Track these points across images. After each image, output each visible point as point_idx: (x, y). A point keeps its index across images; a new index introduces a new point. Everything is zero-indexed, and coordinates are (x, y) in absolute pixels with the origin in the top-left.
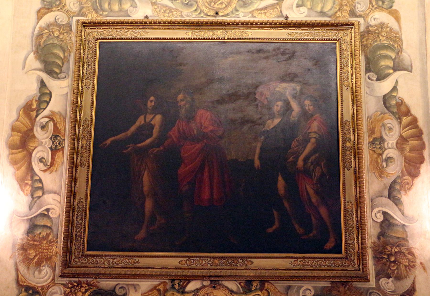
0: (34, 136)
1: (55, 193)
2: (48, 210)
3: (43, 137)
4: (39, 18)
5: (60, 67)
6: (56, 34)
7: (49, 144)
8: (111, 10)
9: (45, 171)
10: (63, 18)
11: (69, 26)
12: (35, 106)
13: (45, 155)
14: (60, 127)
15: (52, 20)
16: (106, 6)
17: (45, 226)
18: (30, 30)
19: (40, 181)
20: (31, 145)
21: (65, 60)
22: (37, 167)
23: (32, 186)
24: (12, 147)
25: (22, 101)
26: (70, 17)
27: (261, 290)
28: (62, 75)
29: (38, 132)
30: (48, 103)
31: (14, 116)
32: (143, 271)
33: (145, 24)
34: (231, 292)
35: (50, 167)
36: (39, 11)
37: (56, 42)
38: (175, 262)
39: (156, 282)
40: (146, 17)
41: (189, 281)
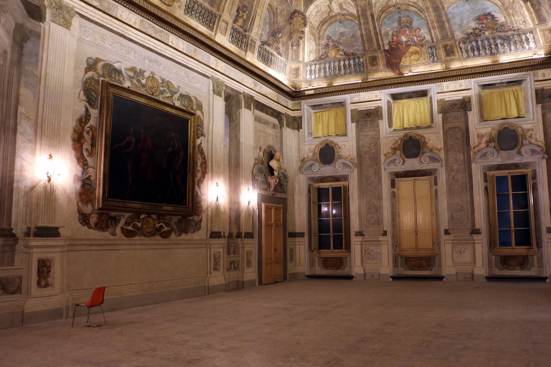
0: (83, 137)
1: (93, 168)
2: (90, 176)
3: (87, 137)
4: (86, 73)
5: (94, 102)
6: (93, 84)
7: (90, 142)
8: (115, 79)
9: (88, 156)
10: (96, 77)
11: (98, 81)
12: (84, 121)
13: (88, 148)
14: (94, 134)
15: (91, 76)
16: (113, 76)
17: (89, 184)
18: (81, 78)
19: (86, 161)
20: (83, 141)
21: (96, 99)
22: (85, 153)
23: (83, 163)
24: (74, 140)
25: (78, 116)
26: (99, 77)
27: (163, 218)
28: (95, 107)
29: (85, 134)
30: (89, 120)
31: (75, 124)
32: (128, 209)
33: (127, 90)
34: (154, 219)
35: (91, 154)
36: (86, 69)
37: (93, 88)
38: (138, 206)
39: (130, 214)
40: (129, 87)
41: (141, 214)
